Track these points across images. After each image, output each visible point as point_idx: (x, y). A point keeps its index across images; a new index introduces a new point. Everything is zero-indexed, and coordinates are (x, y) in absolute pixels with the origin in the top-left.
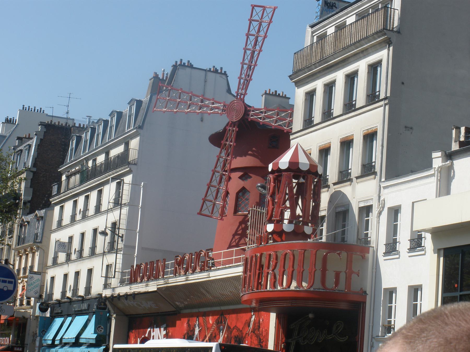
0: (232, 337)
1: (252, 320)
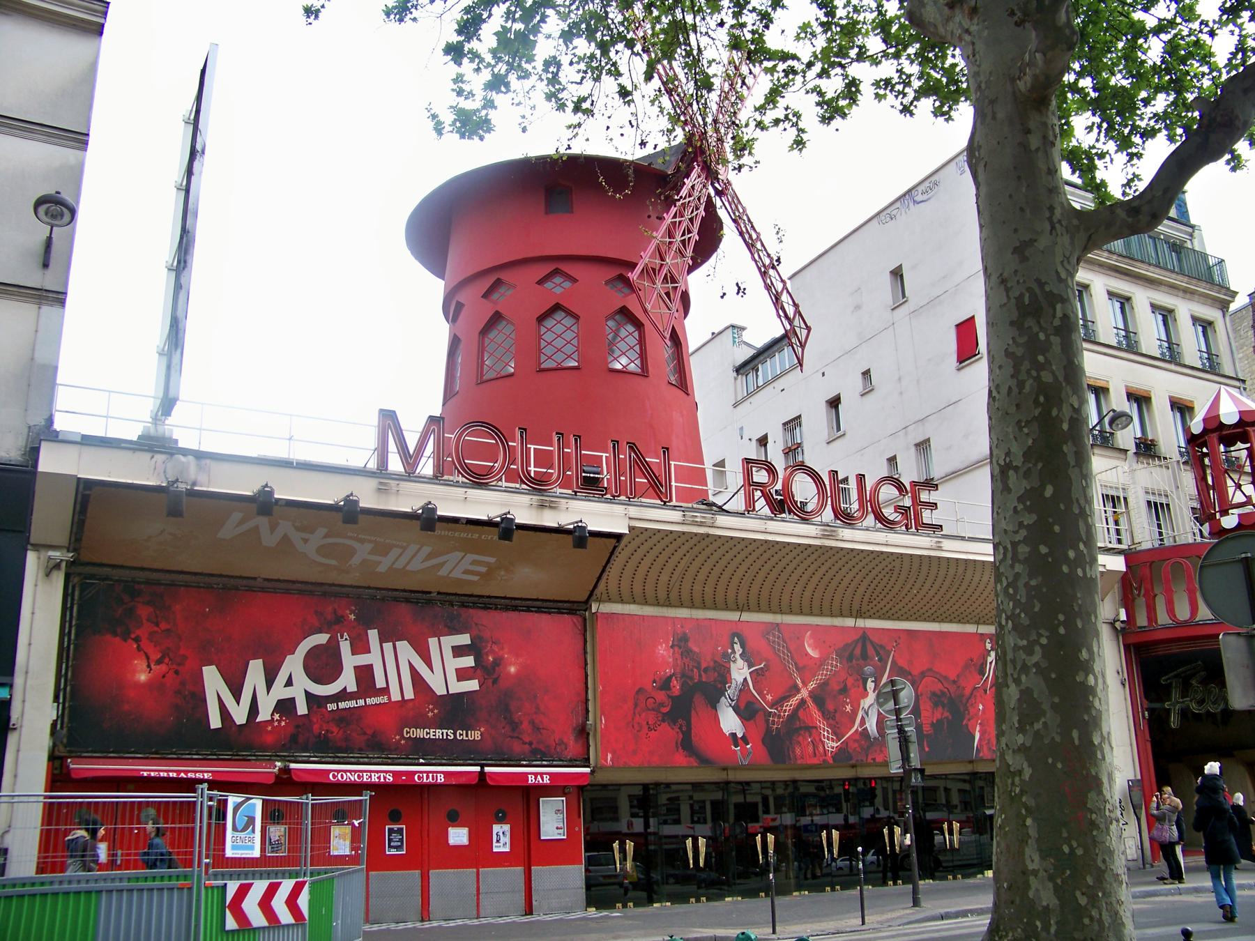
0: (921, 695)
1: (989, 659)
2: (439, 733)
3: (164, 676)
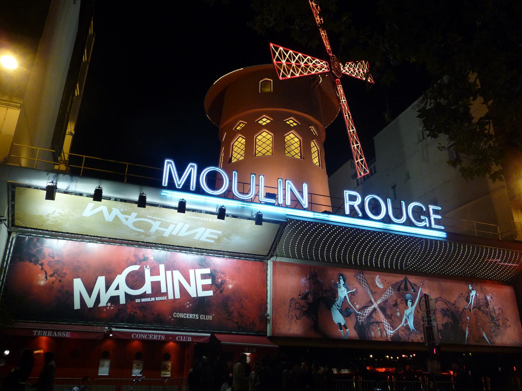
1: (471, 295)
2: (191, 316)
3: (53, 283)
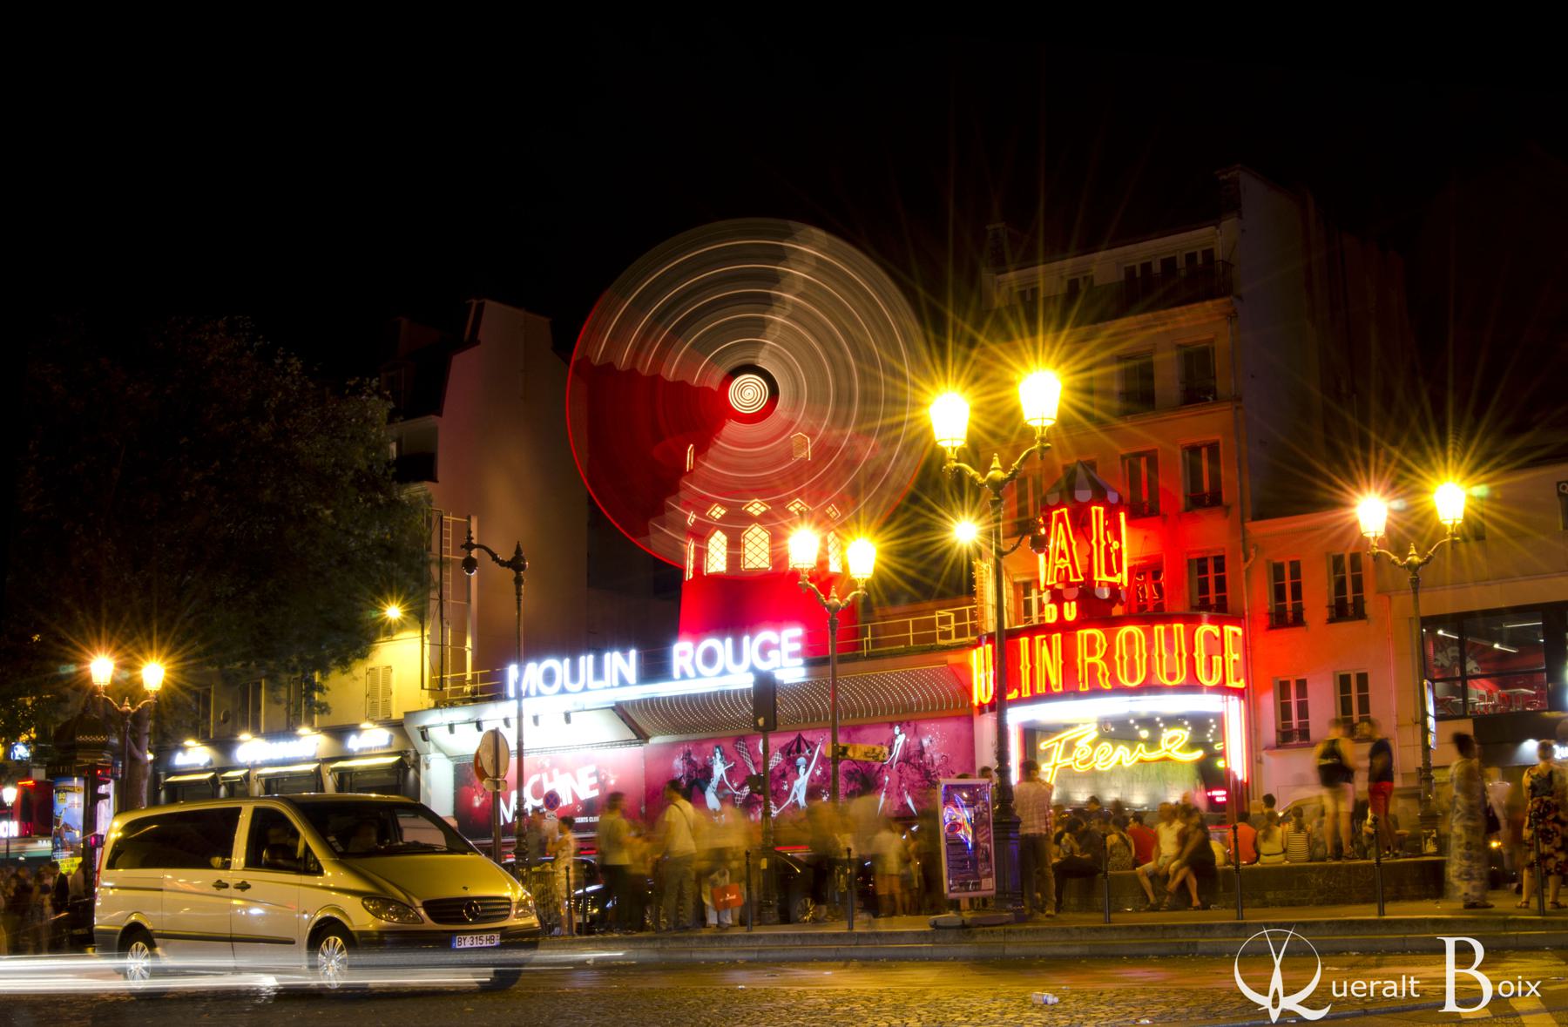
1: (897, 742)
